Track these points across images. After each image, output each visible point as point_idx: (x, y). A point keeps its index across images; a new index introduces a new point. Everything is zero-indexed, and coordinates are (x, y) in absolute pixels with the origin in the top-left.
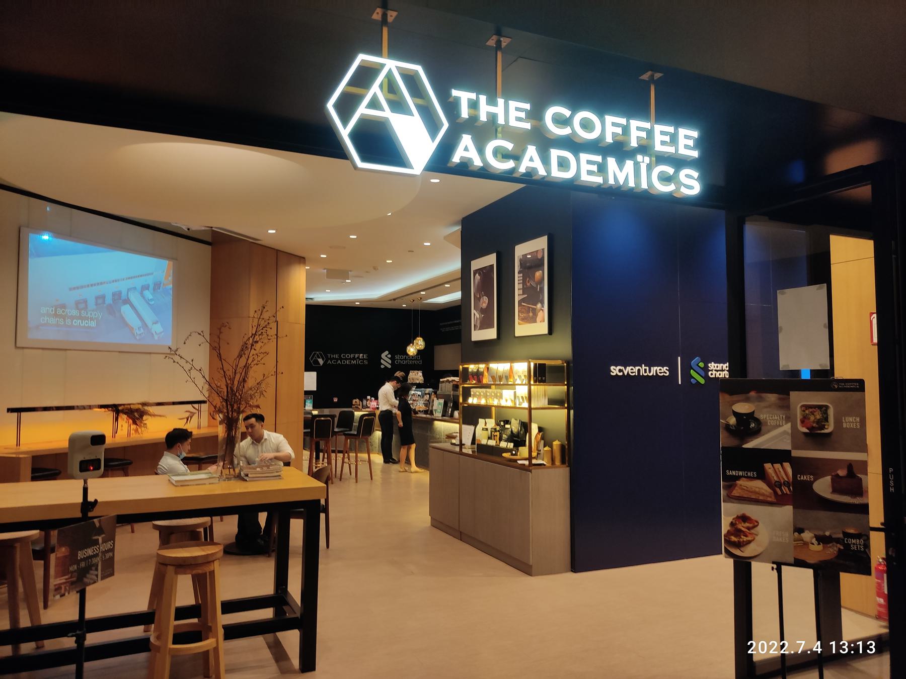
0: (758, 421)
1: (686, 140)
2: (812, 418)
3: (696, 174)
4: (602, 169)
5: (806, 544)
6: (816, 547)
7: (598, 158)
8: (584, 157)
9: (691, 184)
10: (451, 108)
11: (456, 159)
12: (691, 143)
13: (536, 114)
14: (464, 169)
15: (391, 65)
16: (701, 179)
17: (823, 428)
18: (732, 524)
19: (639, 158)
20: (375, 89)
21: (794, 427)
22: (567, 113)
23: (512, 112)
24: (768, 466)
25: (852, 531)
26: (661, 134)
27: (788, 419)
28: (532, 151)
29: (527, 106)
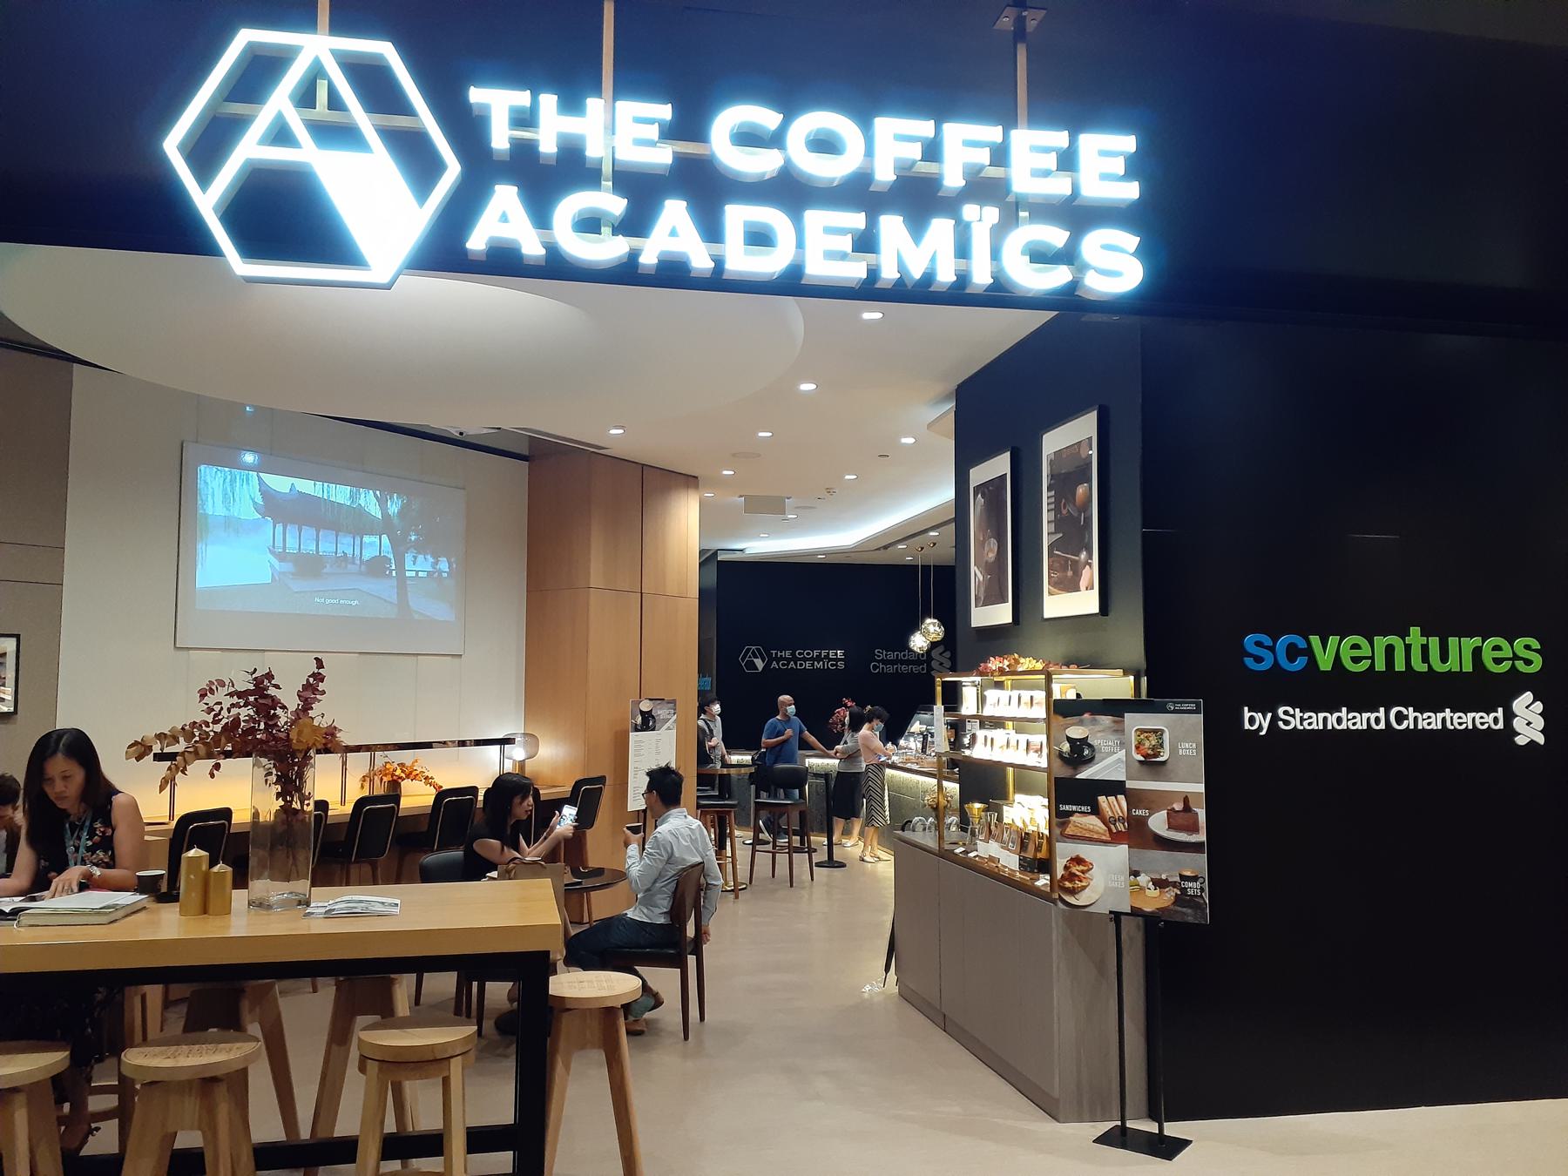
0: (1090, 746)
1: (1107, 161)
2: (1147, 744)
3: (1131, 241)
4: (866, 243)
5: (1142, 889)
6: (1153, 892)
7: (857, 220)
8: (815, 218)
9: (1116, 267)
10: (467, 129)
11: (477, 242)
12: (1119, 166)
13: (689, 125)
14: (503, 263)
15: (317, 48)
16: (1142, 252)
17: (1156, 755)
18: (1066, 868)
19: (970, 211)
20: (279, 101)
21: (1128, 754)
22: (768, 118)
23: (624, 128)
24: (1102, 799)
25: (1188, 873)
26: (1033, 153)
27: (1122, 745)
28: (675, 214)
29: (665, 112)
